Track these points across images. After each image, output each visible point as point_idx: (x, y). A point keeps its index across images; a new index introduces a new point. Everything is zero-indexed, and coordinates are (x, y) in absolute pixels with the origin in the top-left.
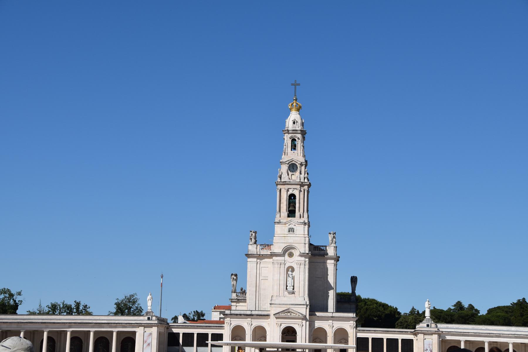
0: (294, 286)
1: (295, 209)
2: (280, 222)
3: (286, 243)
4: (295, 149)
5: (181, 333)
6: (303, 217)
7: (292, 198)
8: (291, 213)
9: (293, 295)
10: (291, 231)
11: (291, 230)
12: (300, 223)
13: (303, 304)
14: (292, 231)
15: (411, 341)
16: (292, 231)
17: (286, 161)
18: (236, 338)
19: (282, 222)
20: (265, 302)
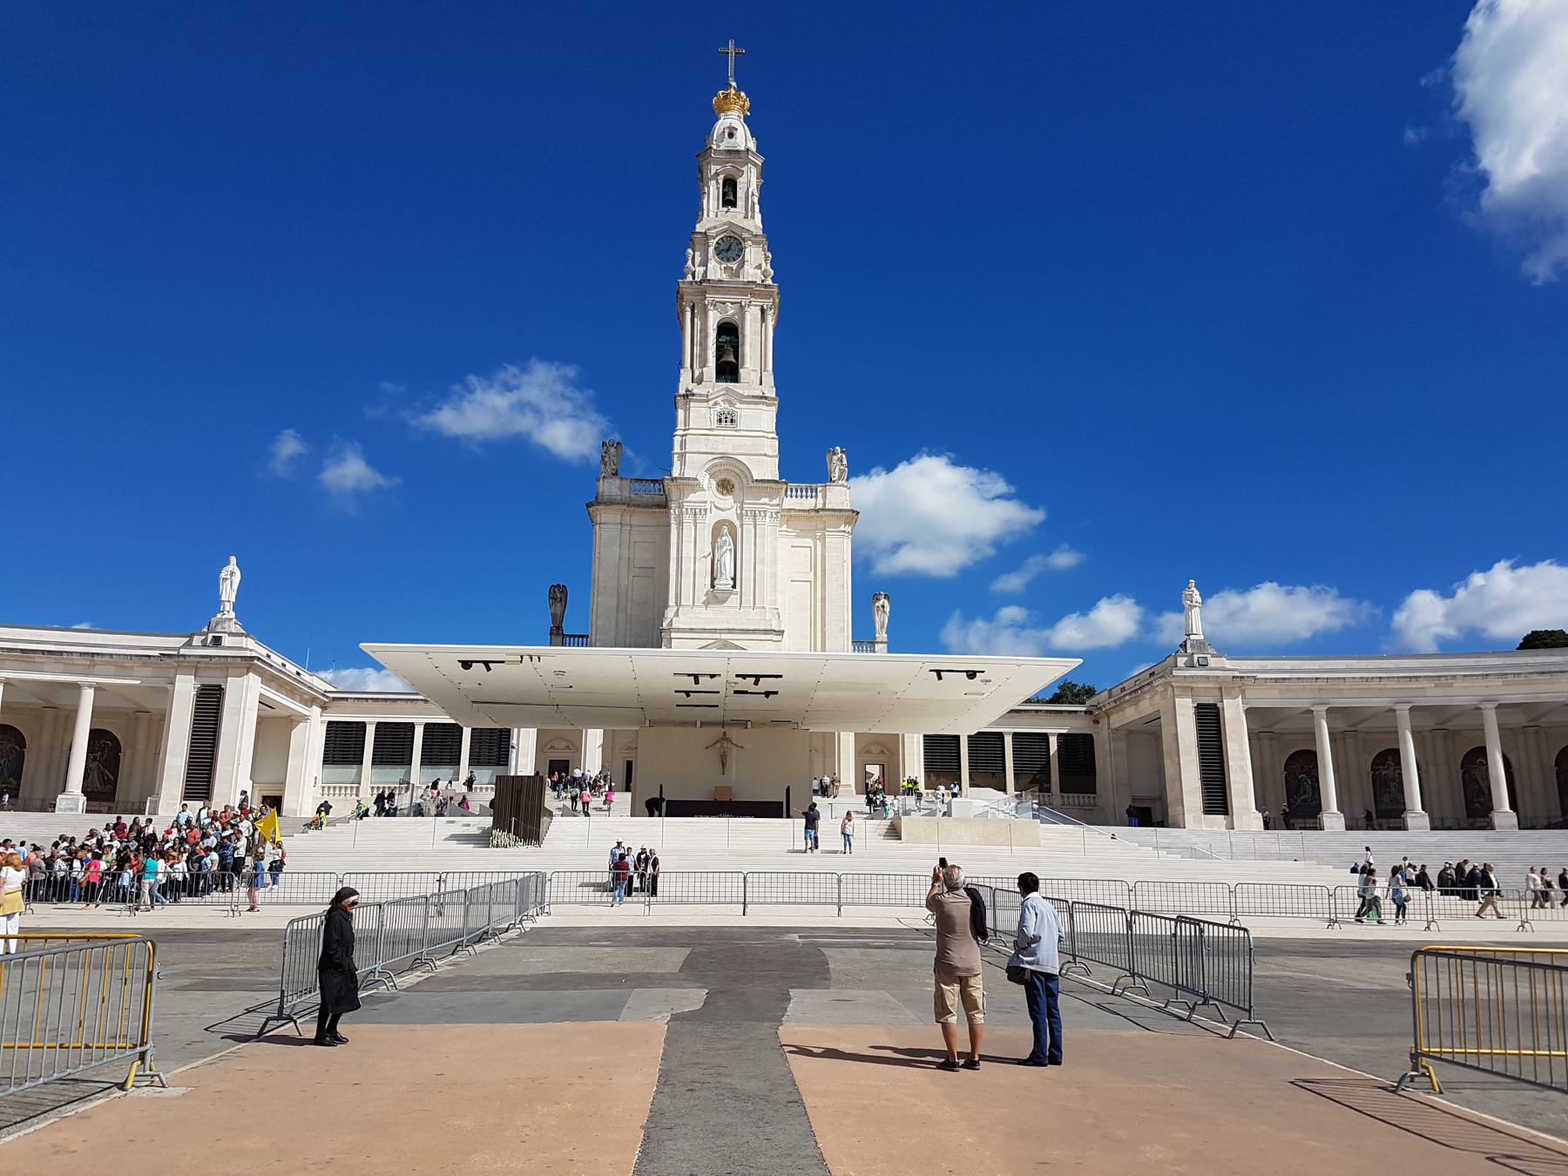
0: (734, 579)
1: (736, 358)
2: (693, 395)
3: (713, 453)
4: (734, 204)
5: (371, 723)
6: (761, 384)
7: (729, 332)
8: (728, 371)
9: (734, 600)
10: (726, 422)
11: (727, 419)
12: (754, 397)
13: (762, 628)
14: (728, 420)
15: (1087, 740)
16: (728, 420)
17: (709, 229)
18: (556, 744)
19: (701, 395)
20: (645, 640)
